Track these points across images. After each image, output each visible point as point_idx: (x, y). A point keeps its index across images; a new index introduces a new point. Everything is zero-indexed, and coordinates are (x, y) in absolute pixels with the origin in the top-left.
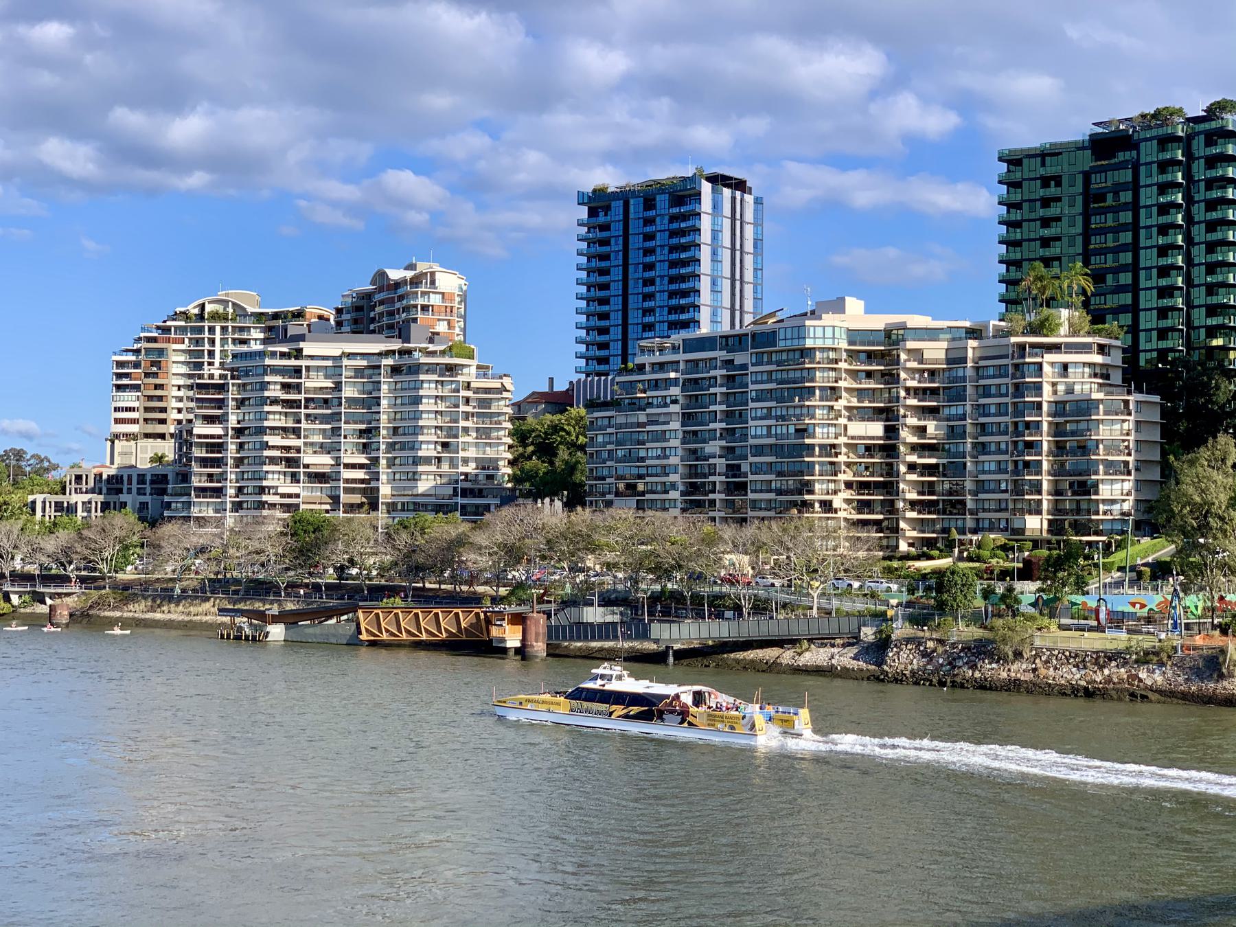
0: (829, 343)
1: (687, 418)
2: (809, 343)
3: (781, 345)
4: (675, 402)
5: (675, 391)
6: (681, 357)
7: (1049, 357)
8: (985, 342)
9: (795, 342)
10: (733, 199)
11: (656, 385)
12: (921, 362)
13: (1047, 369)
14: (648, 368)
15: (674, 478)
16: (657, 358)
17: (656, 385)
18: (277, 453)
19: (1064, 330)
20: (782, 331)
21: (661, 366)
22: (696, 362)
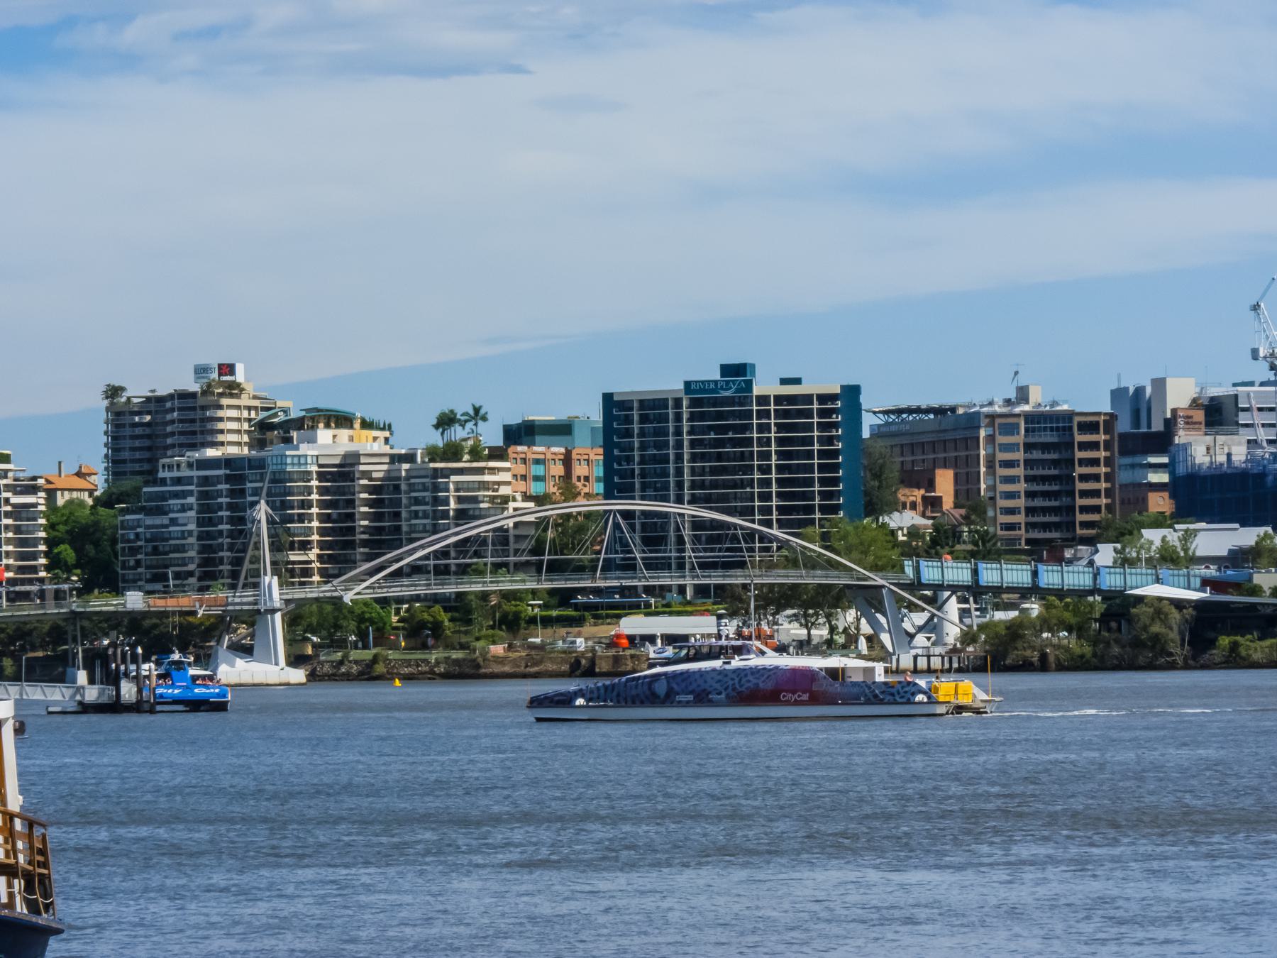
2: (289, 469)
4: (191, 509)
5: (191, 500)
6: (195, 473)
7: (454, 478)
8: (414, 466)
9: (279, 467)
11: (176, 495)
12: (371, 479)
13: (452, 486)
14: (168, 482)
15: (192, 567)
16: (176, 474)
17: (176, 495)
19: (466, 457)
20: (270, 459)
21: (178, 481)
22: (206, 478)
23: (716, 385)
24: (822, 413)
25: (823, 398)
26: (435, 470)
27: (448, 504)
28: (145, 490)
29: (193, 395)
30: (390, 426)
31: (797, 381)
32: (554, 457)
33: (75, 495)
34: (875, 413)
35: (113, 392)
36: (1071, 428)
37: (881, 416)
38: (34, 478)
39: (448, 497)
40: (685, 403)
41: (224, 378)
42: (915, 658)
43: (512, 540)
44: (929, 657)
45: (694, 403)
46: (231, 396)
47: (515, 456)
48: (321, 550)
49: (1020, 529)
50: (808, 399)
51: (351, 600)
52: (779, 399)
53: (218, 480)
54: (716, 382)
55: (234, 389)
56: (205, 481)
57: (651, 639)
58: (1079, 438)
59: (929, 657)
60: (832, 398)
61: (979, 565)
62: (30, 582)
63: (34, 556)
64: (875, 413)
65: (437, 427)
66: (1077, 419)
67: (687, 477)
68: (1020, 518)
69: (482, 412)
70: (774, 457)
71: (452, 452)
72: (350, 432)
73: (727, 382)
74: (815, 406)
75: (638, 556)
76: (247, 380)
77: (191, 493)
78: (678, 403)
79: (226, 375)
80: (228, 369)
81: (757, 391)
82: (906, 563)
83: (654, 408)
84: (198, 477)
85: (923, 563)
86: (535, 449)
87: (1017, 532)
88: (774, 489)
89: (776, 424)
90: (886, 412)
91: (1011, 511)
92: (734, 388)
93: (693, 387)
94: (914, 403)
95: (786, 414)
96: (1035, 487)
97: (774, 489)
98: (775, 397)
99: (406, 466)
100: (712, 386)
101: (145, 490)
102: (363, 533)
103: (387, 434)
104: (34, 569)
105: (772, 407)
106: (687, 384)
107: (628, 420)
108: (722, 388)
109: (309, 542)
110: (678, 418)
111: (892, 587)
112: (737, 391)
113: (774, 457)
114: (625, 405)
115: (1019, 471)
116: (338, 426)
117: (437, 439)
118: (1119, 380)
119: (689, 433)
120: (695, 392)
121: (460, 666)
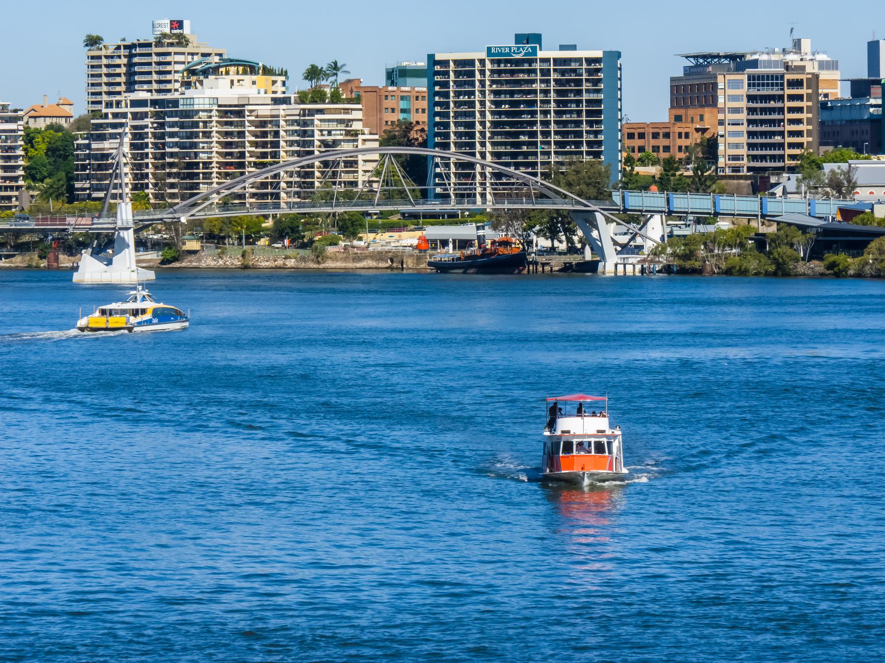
0: (207, 107)
1: (133, 146)
2: (196, 107)
3: (181, 108)
11: (114, 126)
13: (316, 122)
17: (114, 126)
23: (510, 50)
24: (589, 72)
25: (590, 61)
26: (304, 110)
27: (313, 136)
28: (92, 121)
29: (149, 45)
30: (286, 72)
31: (573, 48)
32: (418, 94)
33: (54, 120)
34: (687, 57)
35: (93, 41)
36: (782, 84)
37: (692, 59)
38: (16, 111)
39: (313, 131)
40: (488, 63)
41: (175, 31)
42: (616, 265)
43: (360, 163)
44: (625, 265)
46: (179, 44)
47: (387, 94)
48: (219, 168)
49: (743, 159)
50: (579, 60)
51: (187, 221)
52: (557, 61)
53: (144, 115)
54: (510, 48)
55: (182, 41)
56: (135, 116)
57: (444, 243)
58: (788, 91)
59: (625, 265)
60: (597, 60)
61: (670, 196)
62: (12, 188)
63: (14, 168)
64: (687, 57)
65: (306, 78)
66: (787, 77)
67: (489, 117)
68: (744, 151)
69: (339, 65)
71: (318, 96)
72: (254, 78)
73: (518, 48)
74: (585, 66)
75: (406, 188)
76: (192, 32)
78: (482, 62)
79: (176, 29)
80: (179, 24)
81: (541, 54)
82: (613, 193)
83: (465, 67)
84: (132, 113)
85: (627, 194)
86: (403, 89)
87: (741, 162)
88: (553, 128)
89: (555, 80)
90: (696, 57)
91: (737, 146)
92: (523, 52)
93: (493, 51)
94: (715, 51)
95: (563, 72)
96: (753, 128)
97: (553, 128)
98: (554, 59)
99: (284, 106)
100: (507, 50)
101: (92, 121)
102: (251, 156)
103: (283, 78)
104: (16, 179)
105: (552, 67)
106: (489, 49)
107: (447, 73)
108: (514, 52)
109: (211, 163)
110: (483, 72)
112: (526, 54)
114: (445, 63)
115: (743, 116)
116: (245, 73)
117: (307, 86)
118: (874, 33)
120: (494, 55)
121: (305, 262)
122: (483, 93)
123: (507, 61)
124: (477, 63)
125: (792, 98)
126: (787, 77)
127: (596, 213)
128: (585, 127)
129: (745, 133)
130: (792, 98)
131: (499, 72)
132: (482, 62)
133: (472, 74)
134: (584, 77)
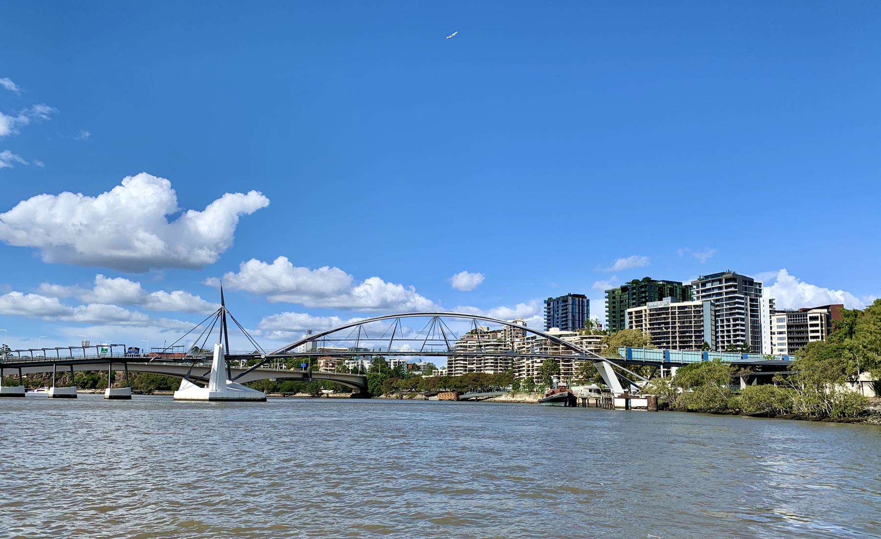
5: (524, 349)
7: (584, 340)
10: (579, 300)
18: (462, 365)
25: (695, 306)
36: (807, 319)
40: (647, 310)
45: (650, 310)
50: (690, 307)
52: (679, 308)
58: (809, 322)
70: (677, 328)
77: (524, 347)
97: (677, 339)
111: (608, 361)
112: (664, 305)
113: (677, 328)
115: (785, 335)
119: (649, 321)
122: (646, 324)
123: (656, 310)
124: (643, 311)
125: (812, 325)
126: (809, 315)
127: (603, 362)
128: (693, 339)
129: (787, 344)
130: (812, 325)
131: (653, 315)
132: (645, 310)
133: (641, 316)
134: (693, 314)
